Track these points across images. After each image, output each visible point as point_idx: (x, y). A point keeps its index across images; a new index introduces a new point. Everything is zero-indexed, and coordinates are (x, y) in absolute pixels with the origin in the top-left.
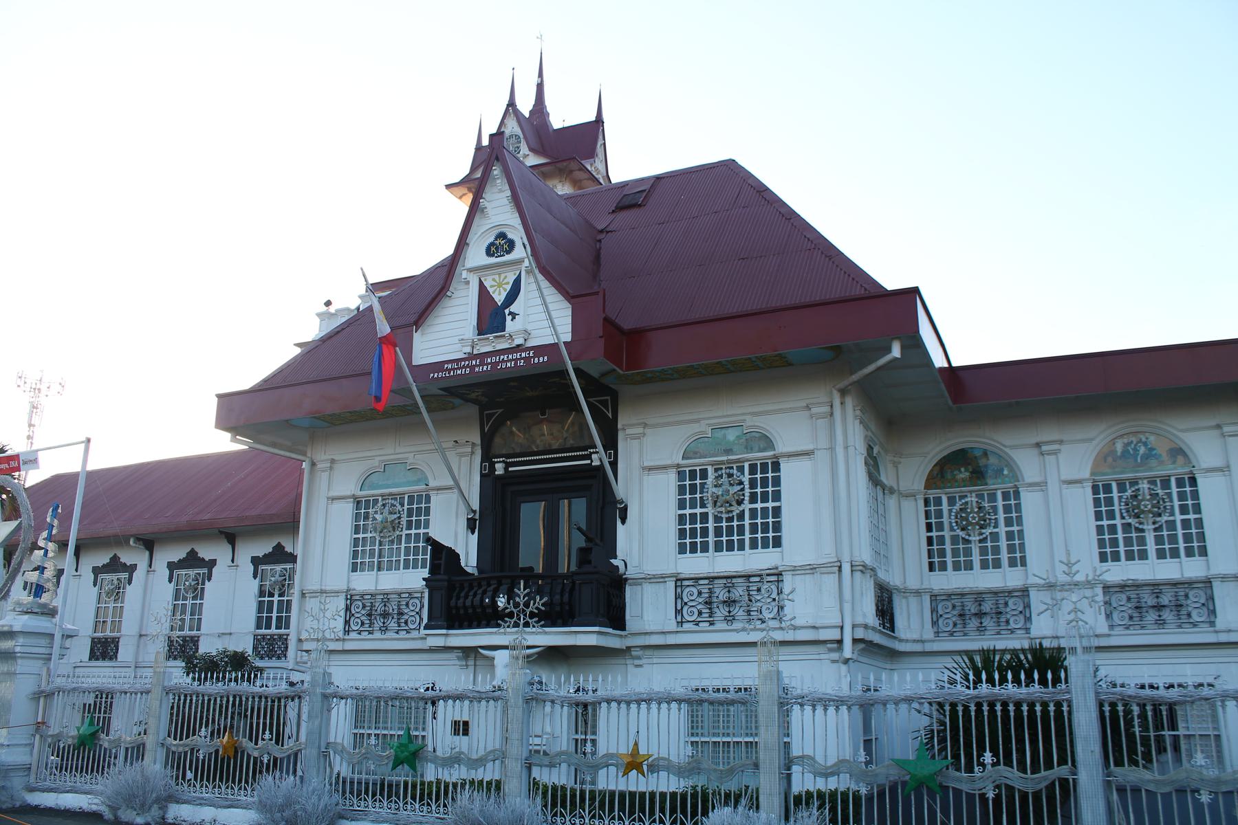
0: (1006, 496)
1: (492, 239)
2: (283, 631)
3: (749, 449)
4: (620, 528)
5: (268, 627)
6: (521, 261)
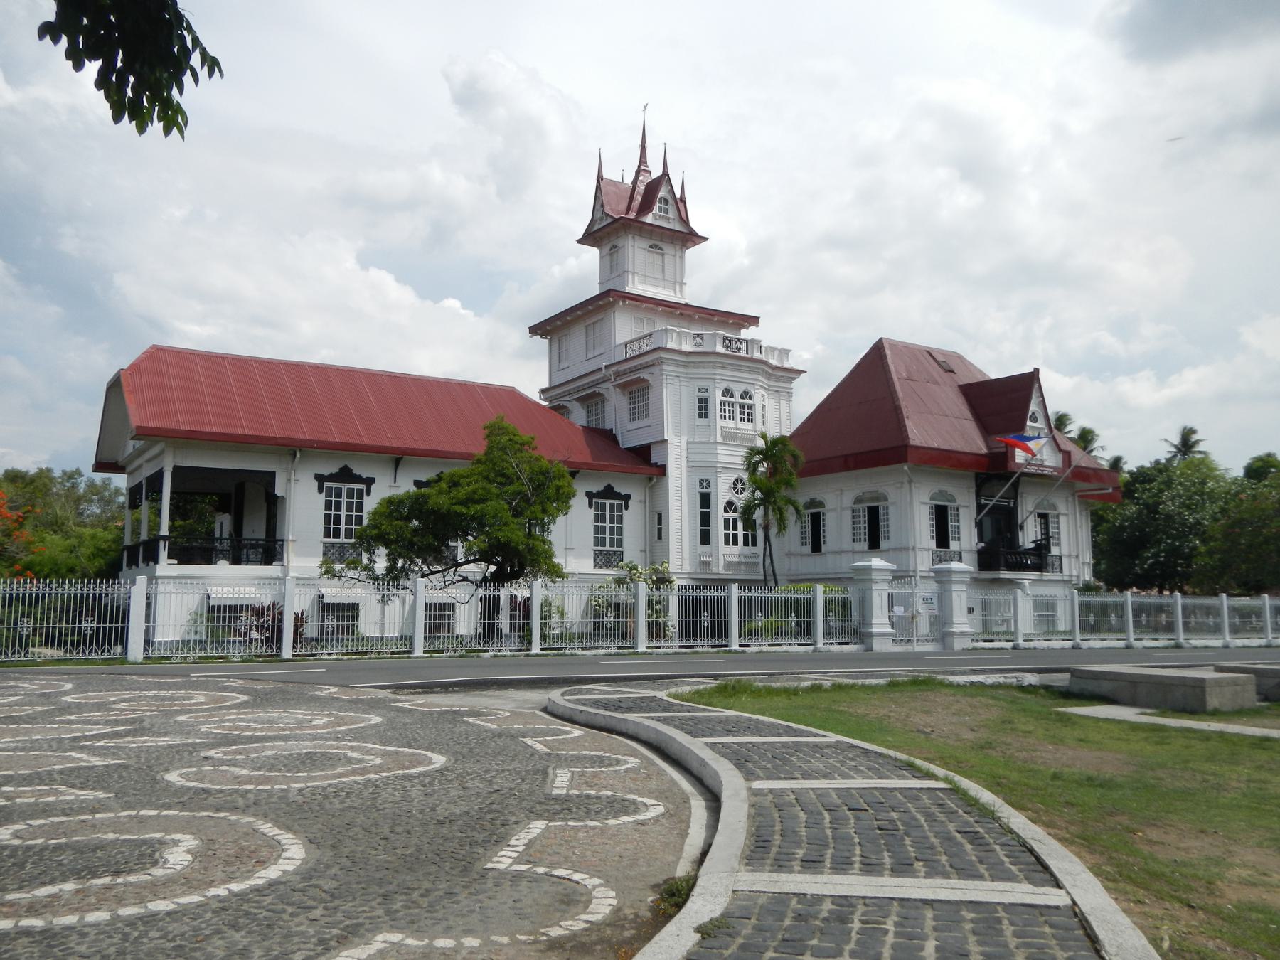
2: (615, 549)
4: (1020, 534)
5: (603, 544)
6: (1042, 429)
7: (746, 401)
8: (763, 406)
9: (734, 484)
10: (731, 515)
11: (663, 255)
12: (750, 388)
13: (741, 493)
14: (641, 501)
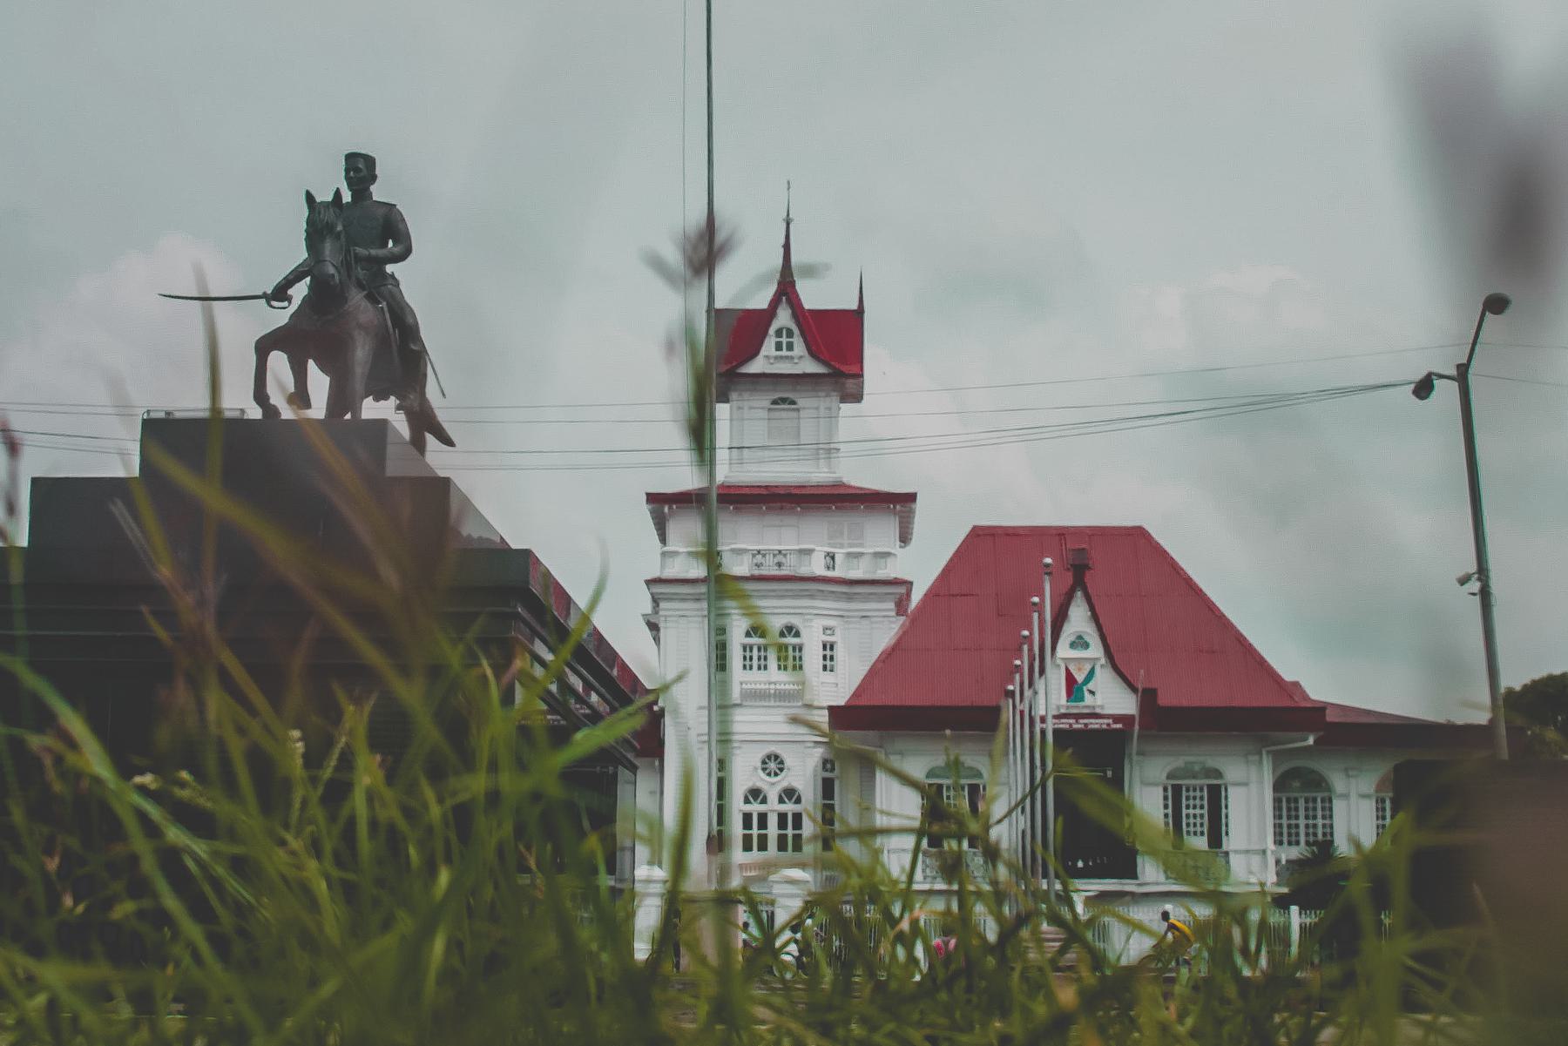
0: (1323, 801)
1: (1073, 638)
3: (1207, 776)
7: (791, 640)
8: (828, 646)
9: (764, 762)
10: (755, 808)
11: (798, 410)
12: (795, 621)
13: (776, 774)
14: (652, 793)
